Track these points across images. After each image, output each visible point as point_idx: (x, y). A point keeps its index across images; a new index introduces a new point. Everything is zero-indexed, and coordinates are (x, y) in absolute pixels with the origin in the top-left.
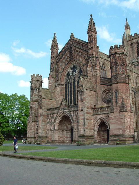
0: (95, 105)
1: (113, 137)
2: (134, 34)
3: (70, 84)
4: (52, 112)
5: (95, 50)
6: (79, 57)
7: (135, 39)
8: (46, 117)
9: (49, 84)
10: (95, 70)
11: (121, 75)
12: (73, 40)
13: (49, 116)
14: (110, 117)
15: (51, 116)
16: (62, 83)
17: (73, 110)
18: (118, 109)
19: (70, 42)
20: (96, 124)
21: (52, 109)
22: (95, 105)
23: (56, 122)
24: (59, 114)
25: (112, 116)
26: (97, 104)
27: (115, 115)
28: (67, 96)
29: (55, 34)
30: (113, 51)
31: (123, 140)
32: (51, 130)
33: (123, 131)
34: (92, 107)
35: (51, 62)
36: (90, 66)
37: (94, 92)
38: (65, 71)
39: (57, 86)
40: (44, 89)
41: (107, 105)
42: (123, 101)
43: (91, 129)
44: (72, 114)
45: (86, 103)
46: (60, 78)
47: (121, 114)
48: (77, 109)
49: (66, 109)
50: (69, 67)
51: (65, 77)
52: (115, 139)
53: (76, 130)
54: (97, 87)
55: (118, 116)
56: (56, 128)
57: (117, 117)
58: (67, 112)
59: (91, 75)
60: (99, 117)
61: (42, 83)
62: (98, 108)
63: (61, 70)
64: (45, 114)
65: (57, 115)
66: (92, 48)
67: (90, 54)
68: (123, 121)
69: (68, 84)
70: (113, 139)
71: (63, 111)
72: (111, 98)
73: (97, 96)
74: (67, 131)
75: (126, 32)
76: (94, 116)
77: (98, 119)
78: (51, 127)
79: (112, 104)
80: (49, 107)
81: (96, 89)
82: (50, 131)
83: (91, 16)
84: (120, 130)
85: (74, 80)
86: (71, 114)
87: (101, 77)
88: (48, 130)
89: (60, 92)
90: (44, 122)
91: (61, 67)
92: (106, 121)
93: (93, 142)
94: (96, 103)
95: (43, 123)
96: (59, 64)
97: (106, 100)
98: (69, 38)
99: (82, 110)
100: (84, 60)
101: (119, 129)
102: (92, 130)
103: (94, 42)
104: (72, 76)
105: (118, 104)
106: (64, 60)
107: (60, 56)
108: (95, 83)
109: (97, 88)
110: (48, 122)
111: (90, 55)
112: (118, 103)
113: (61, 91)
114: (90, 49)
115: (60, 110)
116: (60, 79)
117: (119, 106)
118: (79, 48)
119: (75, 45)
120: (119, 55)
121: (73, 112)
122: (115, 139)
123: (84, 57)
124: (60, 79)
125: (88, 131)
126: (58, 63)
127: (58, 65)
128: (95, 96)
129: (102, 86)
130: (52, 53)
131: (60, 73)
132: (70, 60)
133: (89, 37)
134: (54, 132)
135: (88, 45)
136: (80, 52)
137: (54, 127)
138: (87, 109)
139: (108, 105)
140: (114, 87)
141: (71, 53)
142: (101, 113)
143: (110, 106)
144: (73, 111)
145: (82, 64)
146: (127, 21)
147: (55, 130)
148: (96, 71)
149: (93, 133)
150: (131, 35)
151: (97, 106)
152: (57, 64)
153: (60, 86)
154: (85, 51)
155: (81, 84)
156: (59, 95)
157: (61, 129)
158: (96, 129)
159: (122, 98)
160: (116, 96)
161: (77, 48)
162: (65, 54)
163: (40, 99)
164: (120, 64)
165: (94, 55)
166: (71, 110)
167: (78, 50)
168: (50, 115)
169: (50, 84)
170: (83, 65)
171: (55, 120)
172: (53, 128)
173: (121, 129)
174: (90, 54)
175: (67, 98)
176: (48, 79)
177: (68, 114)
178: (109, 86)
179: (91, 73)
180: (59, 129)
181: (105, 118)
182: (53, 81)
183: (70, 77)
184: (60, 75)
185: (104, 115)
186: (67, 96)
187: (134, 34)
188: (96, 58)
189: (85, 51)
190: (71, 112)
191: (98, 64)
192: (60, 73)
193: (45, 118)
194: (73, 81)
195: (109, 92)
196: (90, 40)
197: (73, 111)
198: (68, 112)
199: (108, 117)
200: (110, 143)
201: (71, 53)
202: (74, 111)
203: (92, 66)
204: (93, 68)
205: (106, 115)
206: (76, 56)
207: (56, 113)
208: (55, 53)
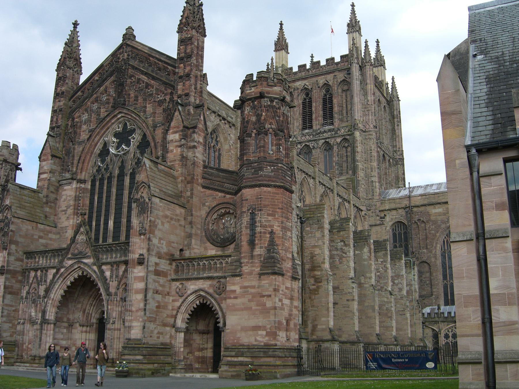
0: (181, 250)
1: (233, 353)
2: (300, 67)
3: (106, 182)
4: (42, 262)
5: (196, 85)
6: (145, 100)
7: (298, 80)
8: (20, 278)
9: (40, 174)
10: (192, 144)
11: (272, 163)
12: (129, 49)
13: (28, 277)
14: (230, 288)
15: (36, 276)
16: (82, 176)
17: (109, 260)
18: (257, 265)
19: (120, 54)
20: (183, 309)
21: (43, 253)
22: (181, 250)
23: (52, 296)
24: (62, 270)
25: (237, 288)
26: (189, 245)
27: (246, 284)
28: (95, 215)
29: (75, 24)
30: (253, 89)
31: (266, 366)
32: (33, 323)
33: (268, 334)
34: (173, 255)
35: (53, 107)
36: (175, 130)
37: (179, 211)
38: (96, 139)
39: (65, 182)
40: (22, 188)
41: (220, 253)
42: (272, 243)
43: (165, 325)
44: (108, 274)
45: (155, 241)
46: (76, 158)
47: (266, 281)
48: (123, 259)
49: (88, 257)
50: (108, 128)
51: (93, 159)
52: (240, 359)
53: (117, 326)
54: (192, 194)
55: (253, 287)
56: (51, 315)
57: (253, 291)
58: (89, 266)
59: (178, 157)
60: (192, 286)
61: (18, 172)
62: (191, 259)
63: (84, 136)
64: (18, 269)
65: (57, 273)
66: (188, 75)
67: (180, 92)
68: (269, 304)
69: (102, 180)
70: (235, 359)
71: (79, 262)
72: (232, 230)
73: (191, 223)
74: (84, 329)
75: (276, 59)
76: (178, 284)
77: (189, 292)
78: (33, 310)
79: (238, 248)
80: (32, 248)
81: (188, 201)
82: (28, 326)
84: (260, 332)
85: (122, 168)
86: (102, 272)
87: (205, 167)
88: (22, 321)
89: (72, 203)
90: (10, 293)
91: (84, 127)
92: (215, 300)
93: (168, 368)
94: (186, 243)
95: (8, 296)
96: (80, 116)
97: (218, 236)
99: (141, 262)
100: (160, 110)
101: (256, 328)
102: (168, 329)
103: (194, 60)
104: (116, 156)
105: (258, 251)
106: (95, 106)
107: (83, 92)
108: (188, 183)
109: (192, 198)
110: (24, 294)
111: (180, 97)
112: (257, 246)
113: (77, 198)
114: (181, 77)
116: (75, 162)
117: (260, 255)
118: (146, 74)
119: (135, 63)
120: (272, 101)
121: (109, 267)
122: (240, 359)
123: (161, 103)
124: (75, 162)
125: (156, 331)
126: (77, 114)
127: (73, 119)
128: (183, 222)
129: (208, 192)
130: (60, 80)
132: (114, 107)
133: (181, 42)
134: (41, 329)
135: (175, 67)
136: (147, 86)
137: (44, 312)
138: (157, 260)
139: (223, 251)
140: (248, 197)
141: (120, 86)
142: (201, 276)
143: (230, 256)
144: (111, 264)
145: (150, 121)
146: (281, 28)
147: (45, 321)
148: (194, 147)
149: (171, 336)
150: (291, 69)
151: (187, 254)
152: (70, 115)
153: (74, 185)
154: (165, 83)
155: (146, 180)
156: (70, 211)
157: (65, 320)
158: (180, 323)
159: (272, 233)
160: (252, 225)
161: (143, 73)
162: (100, 86)
163: (6, 218)
164: (271, 130)
165: (192, 99)
166: (104, 261)
167: (144, 78)
169: (43, 176)
170: (155, 127)
171: (47, 291)
172: (40, 315)
173: (264, 328)
174: (180, 92)
175: (94, 224)
176: (40, 158)
177: (93, 272)
178: (229, 193)
179: (179, 150)
180: (58, 320)
181: (211, 291)
182: (54, 167)
183: (108, 159)
184: (78, 149)
185: (208, 283)
186: (95, 215)
187: (300, 67)
188: (197, 107)
189: (165, 83)
190: (104, 267)
191: (201, 126)
192: (80, 143)
193: (17, 281)
194: (117, 172)
195: (229, 213)
196: (183, 51)
197: (111, 264)
198: (95, 268)
199: (221, 290)
200: (226, 371)
201: (120, 86)
202: (115, 263)
203: (182, 131)
204: (185, 137)
205: (215, 282)
206: (136, 97)
207: (53, 268)
208: (69, 82)
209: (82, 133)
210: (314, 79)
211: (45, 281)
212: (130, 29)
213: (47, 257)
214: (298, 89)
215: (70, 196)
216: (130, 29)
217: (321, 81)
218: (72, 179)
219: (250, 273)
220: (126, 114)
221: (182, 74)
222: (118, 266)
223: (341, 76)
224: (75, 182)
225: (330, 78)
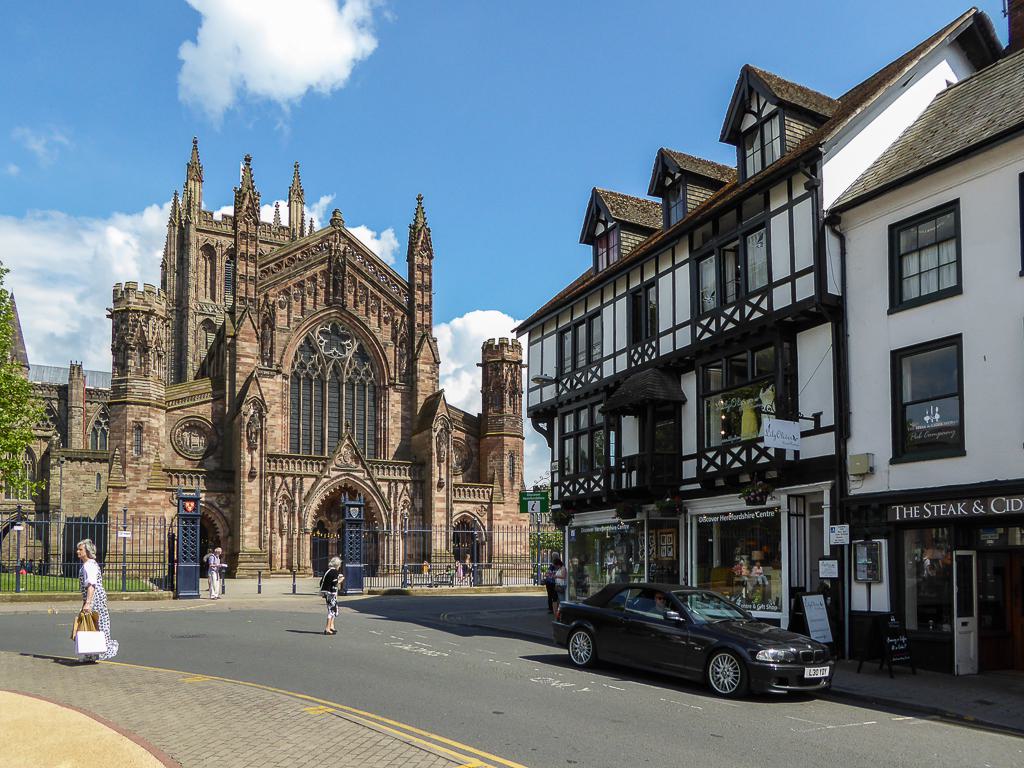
30: (510, 353)
44: (385, 489)
86: (378, 488)
115: (334, 470)
126: (271, 292)
127: (266, 296)
153: (279, 378)
161: (366, 278)
162: (306, 269)
168: (278, 480)
181: (475, 513)
190: (378, 483)
198: (368, 482)
202: (394, 480)
205: (478, 506)
209: (279, 318)
211: (301, 489)
215: (273, 390)
218: (279, 372)
219: (511, 502)
224: (280, 376)
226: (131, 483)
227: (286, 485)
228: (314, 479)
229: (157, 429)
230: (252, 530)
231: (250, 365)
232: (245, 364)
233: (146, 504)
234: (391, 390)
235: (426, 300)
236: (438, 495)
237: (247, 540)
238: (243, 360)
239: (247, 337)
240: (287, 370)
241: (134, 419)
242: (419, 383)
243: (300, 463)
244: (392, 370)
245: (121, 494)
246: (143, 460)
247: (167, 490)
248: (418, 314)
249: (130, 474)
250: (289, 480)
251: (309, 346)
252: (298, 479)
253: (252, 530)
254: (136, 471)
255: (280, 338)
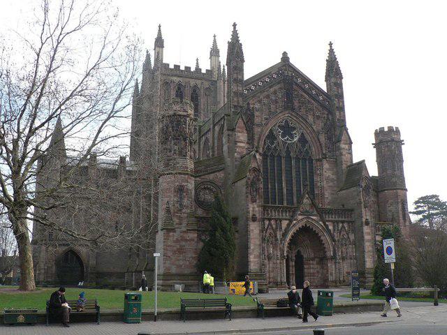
6: (306, 111)
15: (270, 224)
44: (331, 228)
83: (331, 44)
85: (288, 152)
86: (327, 226)
98: (277, 60)
106: (265, 101)
118: (308, 94)
121: (330, 223)
127: (248, 104)
131: (258, 125)
146: (160, 30)
171: (284, 235)
192: (258, 125)
194: (284, 154)
207: (286, 219)
210: (187, 80)
212: (285, 54)
213: (279, 211)
214: (174, 82)
216: (285, 54)
217: (192, 82)
220: (292, 115)
221: (337, 105)
222: (338, 223)
223: (207, 84)
225: (199, 82)
226: (177, 226)
227: (271, 226)
228: (287, 222)
229: (191, 190)
230: (255, 258)
231: (243, 148)
232: (240, 147)
233: (186, 240)
234: (324, 161)
235: (341, 104)
236: (366, 229)
237: (252, 264)
238: (239, 144)
239: (240, 130)
240: (261, 151)
241: (177, 184)
242: (343, 157)
243: (279, 211)
244: (324, 149)
245: (171, 234)
246: (184, 211)
247: (198, 231)
248: (337, 113)
249: (176, 220)
250: (273, 222)
251: (271, 136)
252: (278, 222)
253: (255, 258)
254: (180, 218)
255: (257, 130)
